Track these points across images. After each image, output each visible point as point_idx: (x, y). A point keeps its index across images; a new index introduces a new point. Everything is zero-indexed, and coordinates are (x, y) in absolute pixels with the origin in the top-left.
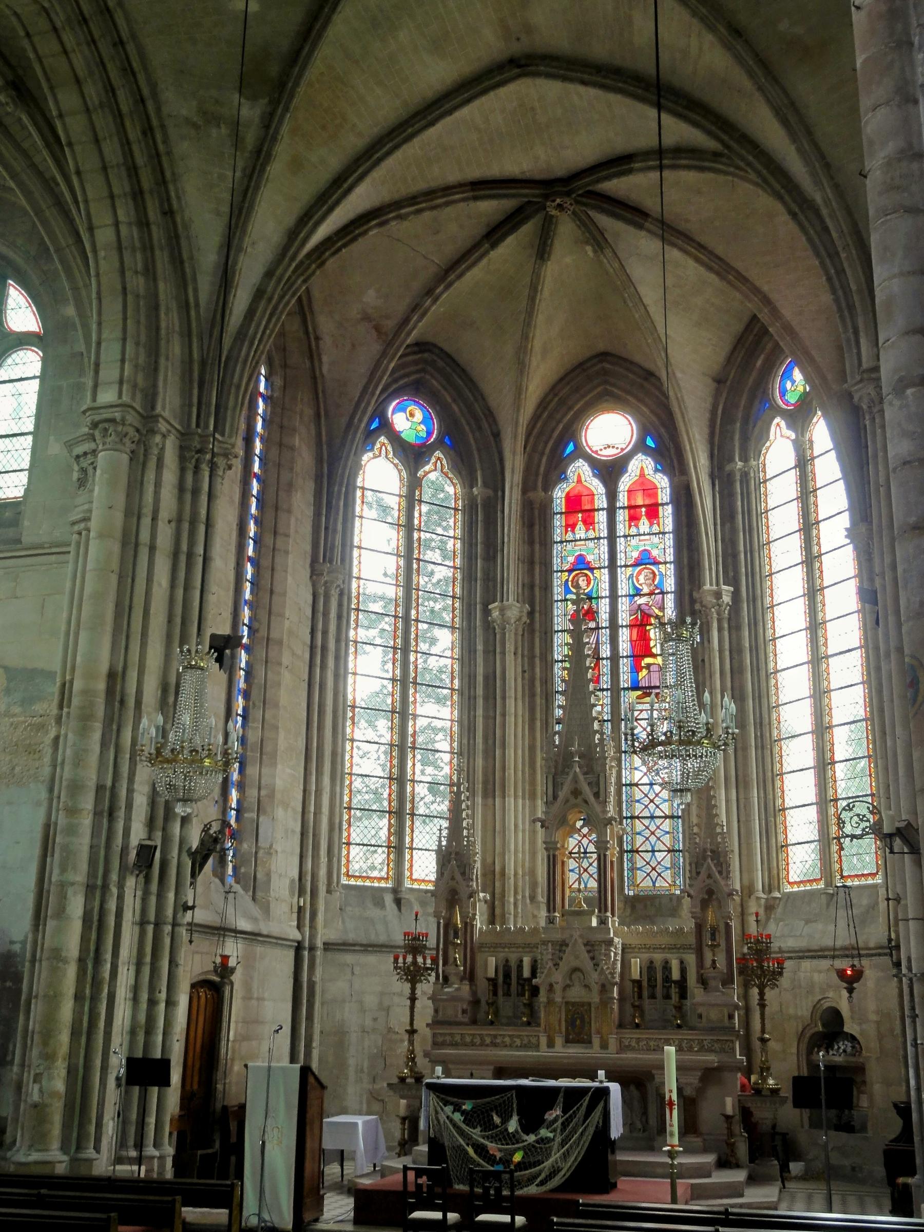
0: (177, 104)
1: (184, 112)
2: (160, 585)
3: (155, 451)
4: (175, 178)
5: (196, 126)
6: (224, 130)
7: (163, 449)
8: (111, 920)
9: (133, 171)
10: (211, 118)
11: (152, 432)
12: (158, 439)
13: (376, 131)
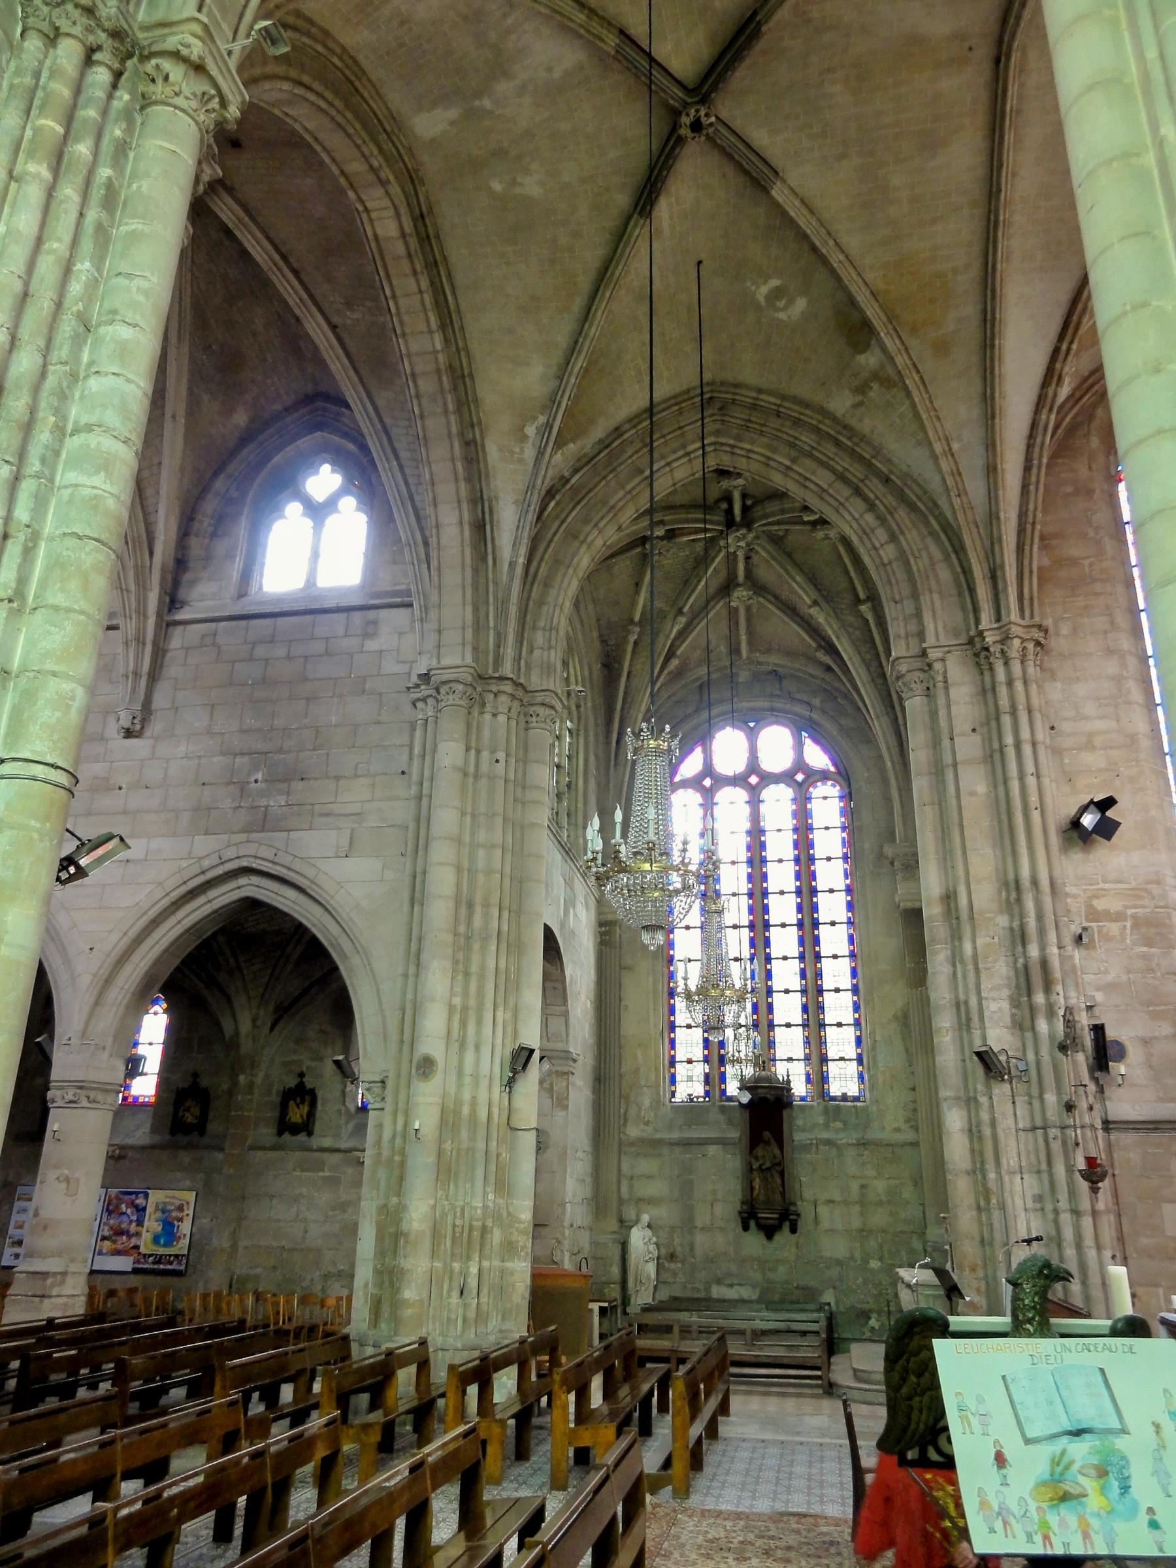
0: (841, 403)
1: (848, 404)
2: (973, 794)
3: (940, 678)
4: (877, 451)
5: (860, 404)
6: (875, 386)
7: (945, 672)
8: (987, 1131)
9: (842, 478)
10: (862, 389)
11: (930, 665)
12: (938, 666)
13: (977, 249)
